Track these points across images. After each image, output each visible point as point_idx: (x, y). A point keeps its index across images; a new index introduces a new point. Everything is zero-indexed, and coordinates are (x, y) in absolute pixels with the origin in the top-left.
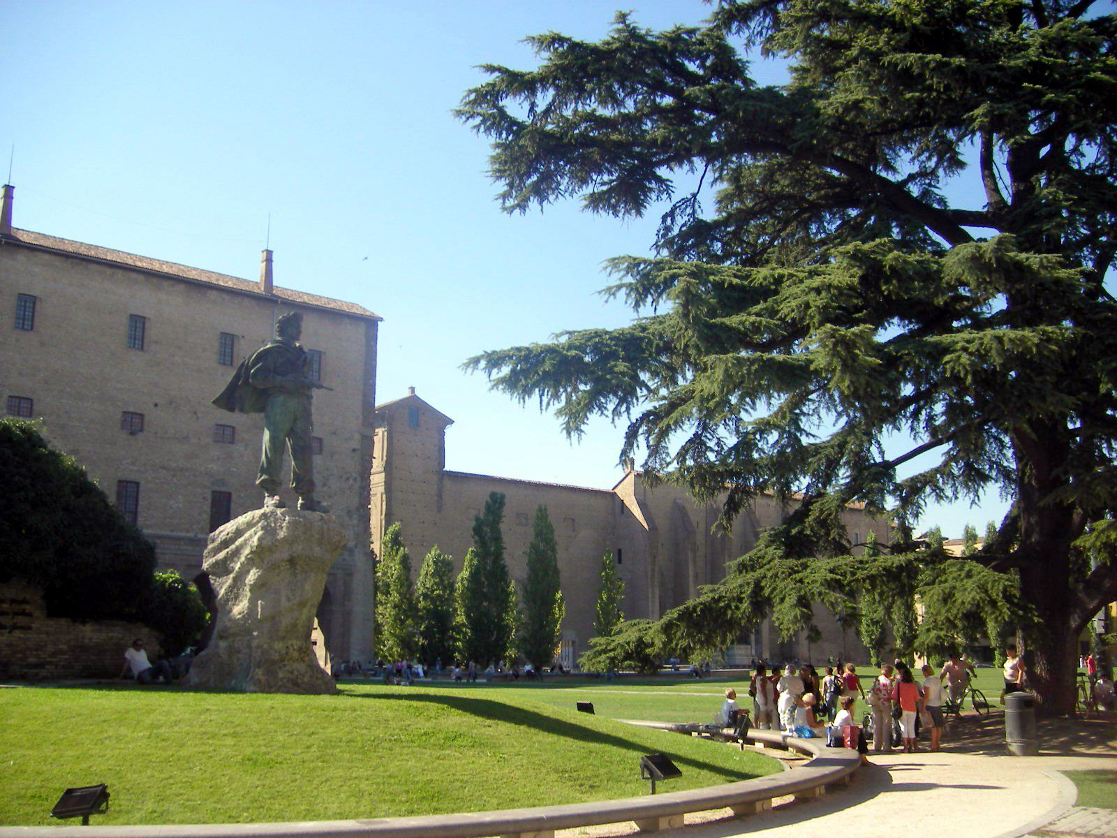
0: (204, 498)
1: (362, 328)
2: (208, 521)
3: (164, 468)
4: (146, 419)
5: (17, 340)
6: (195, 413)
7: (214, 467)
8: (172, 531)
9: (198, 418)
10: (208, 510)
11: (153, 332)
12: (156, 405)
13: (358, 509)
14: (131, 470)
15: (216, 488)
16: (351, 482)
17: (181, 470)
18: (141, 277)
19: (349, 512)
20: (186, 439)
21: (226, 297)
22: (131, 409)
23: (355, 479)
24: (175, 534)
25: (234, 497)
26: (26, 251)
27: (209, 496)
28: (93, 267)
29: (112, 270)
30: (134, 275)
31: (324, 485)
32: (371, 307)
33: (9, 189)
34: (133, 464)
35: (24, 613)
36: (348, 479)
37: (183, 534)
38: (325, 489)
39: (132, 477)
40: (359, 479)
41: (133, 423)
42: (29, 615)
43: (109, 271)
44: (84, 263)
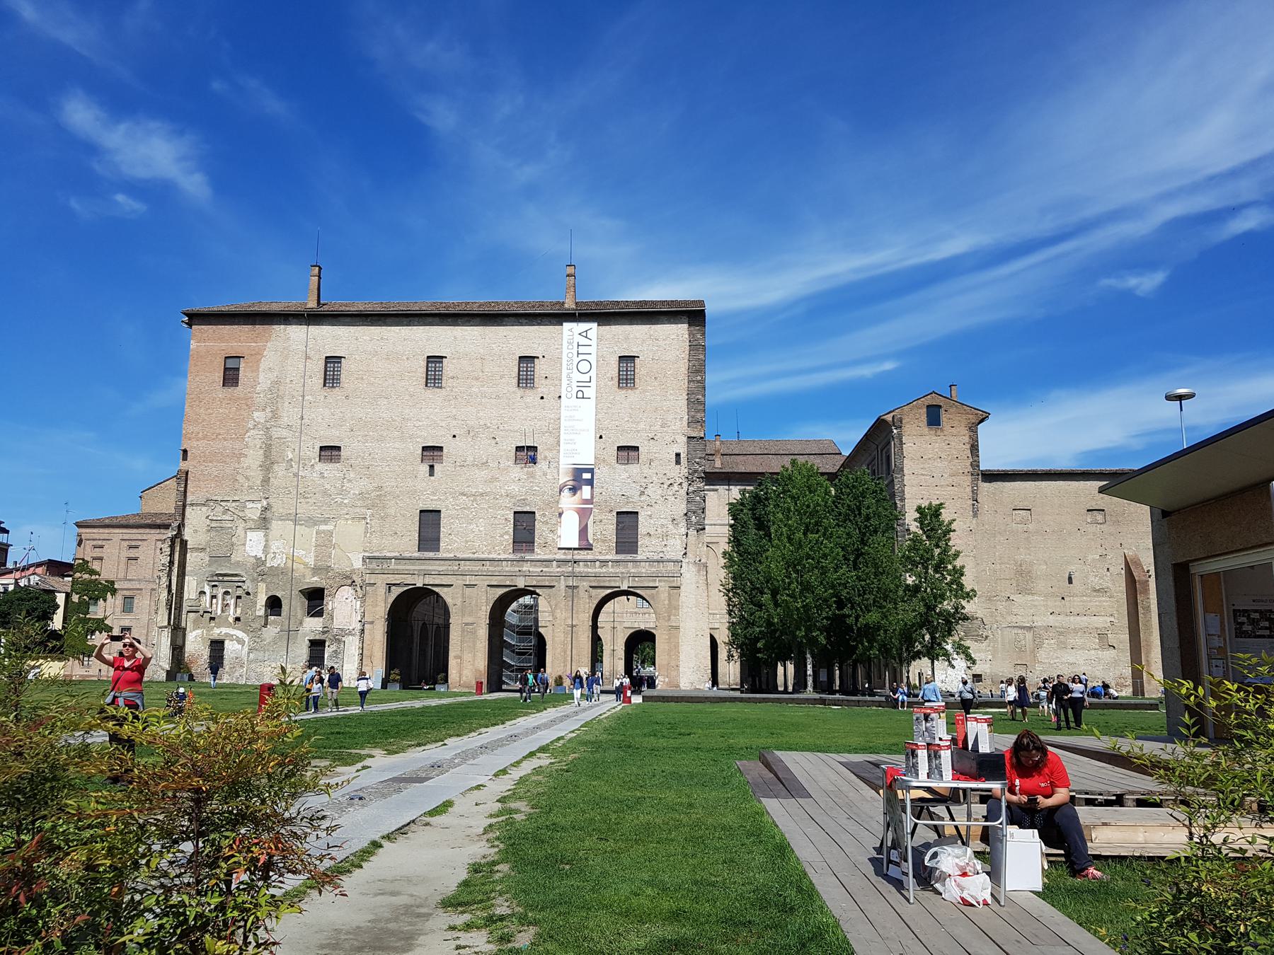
3: (463, 494)
4: (445, 450)
7: (515, 488)
15: (520, 509)
16: (676, 487)
17: (482, 495)
27: (511, 517)
28: (389, 320)
31: (642, 493)
34: (434, 494)
37: (485, 556)
40: (685, 485)
43: (405, 320)
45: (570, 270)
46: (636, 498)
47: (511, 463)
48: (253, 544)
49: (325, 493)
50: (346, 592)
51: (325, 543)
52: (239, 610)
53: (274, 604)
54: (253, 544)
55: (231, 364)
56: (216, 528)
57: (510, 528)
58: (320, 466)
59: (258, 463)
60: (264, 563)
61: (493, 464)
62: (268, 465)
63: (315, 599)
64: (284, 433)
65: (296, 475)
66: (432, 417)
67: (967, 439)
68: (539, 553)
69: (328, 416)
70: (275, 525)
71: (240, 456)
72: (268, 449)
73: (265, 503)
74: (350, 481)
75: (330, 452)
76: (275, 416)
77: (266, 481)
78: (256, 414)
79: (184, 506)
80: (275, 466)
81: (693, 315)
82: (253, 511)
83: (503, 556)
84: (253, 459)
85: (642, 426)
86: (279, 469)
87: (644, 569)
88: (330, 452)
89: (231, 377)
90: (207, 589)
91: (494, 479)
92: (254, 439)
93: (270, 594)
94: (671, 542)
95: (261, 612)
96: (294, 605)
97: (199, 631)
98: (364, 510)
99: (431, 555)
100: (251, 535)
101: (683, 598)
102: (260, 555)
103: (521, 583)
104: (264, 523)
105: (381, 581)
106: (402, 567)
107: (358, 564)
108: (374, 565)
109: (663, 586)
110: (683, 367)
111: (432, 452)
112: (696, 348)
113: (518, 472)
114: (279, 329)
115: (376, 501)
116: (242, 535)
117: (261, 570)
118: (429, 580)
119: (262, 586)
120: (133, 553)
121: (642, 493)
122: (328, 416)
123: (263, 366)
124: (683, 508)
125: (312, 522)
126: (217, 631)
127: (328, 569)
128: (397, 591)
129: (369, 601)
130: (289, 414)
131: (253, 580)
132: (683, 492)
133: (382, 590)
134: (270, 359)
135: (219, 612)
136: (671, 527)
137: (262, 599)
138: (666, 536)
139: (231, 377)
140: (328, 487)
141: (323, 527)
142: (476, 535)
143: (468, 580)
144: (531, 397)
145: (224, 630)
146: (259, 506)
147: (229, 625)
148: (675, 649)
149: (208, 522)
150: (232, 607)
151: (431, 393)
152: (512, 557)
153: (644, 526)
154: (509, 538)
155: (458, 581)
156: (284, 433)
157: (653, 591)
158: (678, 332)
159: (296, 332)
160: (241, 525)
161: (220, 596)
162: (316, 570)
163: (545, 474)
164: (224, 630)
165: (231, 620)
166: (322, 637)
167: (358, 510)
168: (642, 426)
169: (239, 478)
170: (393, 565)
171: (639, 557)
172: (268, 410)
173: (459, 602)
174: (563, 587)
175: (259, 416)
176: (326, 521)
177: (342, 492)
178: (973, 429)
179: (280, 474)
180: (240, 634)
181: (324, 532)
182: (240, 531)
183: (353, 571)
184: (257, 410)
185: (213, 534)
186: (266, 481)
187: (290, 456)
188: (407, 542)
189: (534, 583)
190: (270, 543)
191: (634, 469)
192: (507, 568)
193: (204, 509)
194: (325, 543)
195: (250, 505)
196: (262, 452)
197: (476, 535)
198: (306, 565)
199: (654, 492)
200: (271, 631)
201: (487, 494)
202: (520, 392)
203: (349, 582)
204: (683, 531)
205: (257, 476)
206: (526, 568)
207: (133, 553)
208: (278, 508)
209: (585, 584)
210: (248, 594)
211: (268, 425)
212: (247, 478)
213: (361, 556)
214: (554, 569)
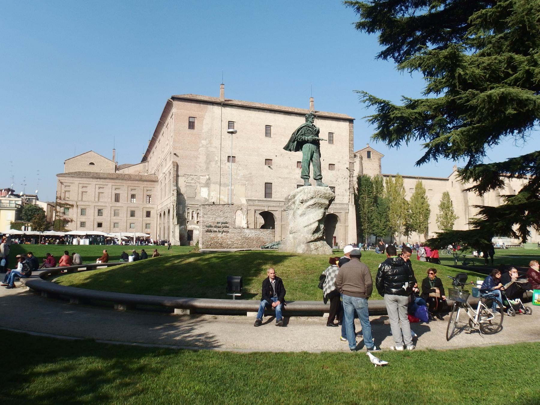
1: (347, 124)
3: (280, 177)
16: (346, 179)
34: (270, 177)
35: (226, 227)
38: (337, 182)
42: (228, 227)
45: (311, 99)
46: (335, 182)
51: (232, 193)
54: (204, 193)
55: (191, 120)
56: (188, 186)
58: (228, 164)
60: (208, 200)
62: (208, 162)
64: (214, 150)
67: (378, 163)
69: (230, 145)
70: (212, 186)
71: (197, 158)
73: (208, 177)
75: (231, 158)
76: (210, 142)
77: (207, 168)
78: (203, 141)
79: (177, 176)
81: (351, 121)
82: (203, 180)
84: (202, 159)
85: (336, 157)
86: (213, 164)
88: (231, 158)
89: (191, 125)
91: (290, 173)
92: (202, 150)
94: (345, 197)
98: (245, 182)
99: (269, 199)
100: (202, 189)
102: (207, 197)
104: (207, 185)
105: (253, 209)
107: (244, 201)
108: (250, 203)
109: (343, 212)
111: (268, 161)
112: (351, 132)
114: (210, 107)
115: (249, 179)
122: (230, 145)
123: (205, 122)
125: (226, 185)
130: (216, 142)
134: (207, 120)
135: (191, 219)
138: (343, 195)
139: (191, 125)
146: (205, 178)
147: (194, 224)
151: (267, 139)
155: (280, 209)
158: (346, 125)
159: (217, 109)
160: (199, 185)
165: (196, 222)
168: (336, 157)
169: (198, 167)
170: (257, 203)
172: (207, 140)
173: (280, 217)
175: (204, 142)
178: (380, 159)
179: (213, 166)
182: (198, 188)
183: (242, 205)
185: (188, 188)
186: (207, 168)
187: (217, 159)
188: (260, 194)
193: (183, 178)
194: (232, 193)
195: (201, 177)
199: (340, 180)
204: (348, 194)
208: (213, 179)
211: (208, 146)
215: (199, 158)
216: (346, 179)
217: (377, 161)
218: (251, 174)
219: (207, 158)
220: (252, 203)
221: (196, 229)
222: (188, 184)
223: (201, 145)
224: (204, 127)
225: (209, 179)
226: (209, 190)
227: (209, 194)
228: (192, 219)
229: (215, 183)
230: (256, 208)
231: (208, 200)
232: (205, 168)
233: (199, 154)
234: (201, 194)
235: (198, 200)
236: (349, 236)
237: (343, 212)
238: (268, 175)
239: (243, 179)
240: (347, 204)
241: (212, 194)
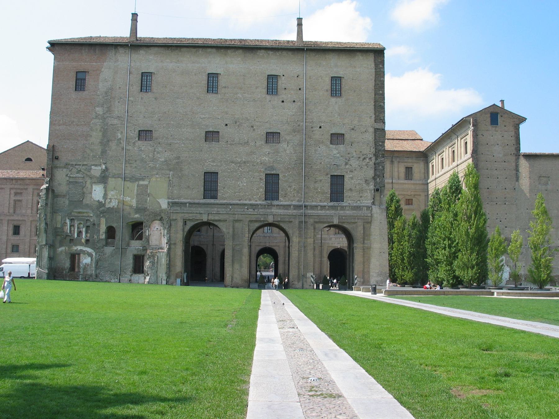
0: (260, 179)
2: (264, 192)
3: (232, 162)
4: (221, 134)
5: (142, 98)
6: (252, 127)
8: (240, 200)
9: (254, 130)
10: (264, 186)
11: (222, 81)
12: (226, 125)
13: (374, 178)
14: (212, 166)
15: (269, 172)
16: (367, 160)
17: (245, 162)
18: (214, 50)
19: (366, 181)
20: (247, 143)
21: (271, 53)
22: (211, 129)
23: (370, 158)
24: (241, 202)
25: (280, 176)
26: (145, 49)
27: (263, 177)
28: (183, 49)
29: (196, 49)
30: (209, 50)
31: (346, 164)
32: (383, 44)
33: (135, 17)
34: (213, 162)
36: (364, 158)
37: (247, 202)
38: (347, 167)
39: (213, 170)
40: (374, 158)
41: (211, 136)
44: (179, 48)
46: (343, 166)
47: (263, 142)
48: (97, 193)
49: (142, 160)
50: (156, 225)
51: (143, 192)
52: (88, 235)
53: (111, 232)
54: (97, 193)
55: (80, 76)
56: (73, 183)
57: (263, 184)
59: (99, 140)
60: (104, 205)
61: (252, 144)
62: (105, 143)
63: (137, 229)
64: (116, 121)
65: (123, 149)
66: (211, 111)
68: (282, 201)
69: (143, 111)
70: (111, 182)
72: (105, 132)
73: (104, 167)
74: (158, 153)
75: (145, 134)
76: (109, 110)
77: (104, 152)
78: (97, 109)
80: (110, 143)
82: (96, 171)
83: (259, 202)
84: (96, 137)
86: (113, 145)
87: (348, 212)
88: (145, 134)
90: (68, 222)
93: (109, 225)
95: (103, 237)
96: (122, 233)
97: (63, 248)
98: (168, 172)
99: (212, 201)
100: (95, 187)
101: (372, 230)
102: (101, 199)
103: (270, 219)
104: (103, 179)
105: (179, 218)
106: (193, 209)
110: (371, 84)
113: (267, 149)
114: (111, 53)
115: (175, 167)
116: (90, 187)
117: (101, 209)
118: (211, 217)
119: (103, 221)
120: (18, 198)
121: (346, 164)
124: (371, 173)
125: (133, 179)
126: (75, 248)
127: (145, 209)
128: (190, 225)
129: (173, 230)
130: (118, 109)
131: (98, 216)
132: (372, 163)
133: (180, 224)
135: (76, 236)
136: (364, 185)
137: (103, 228)
138: (361, 191)
140: (144, 156)
141: (141, 183)
142: (242, 189)
143: (237, 217)
144: (276, 100)
145: (79, 248)
147: (82, 245)
148: (366, 260)
149: (68, 178)
150: (84, 233)
151: (211, 97)
152: (264, 203)
153: (348, 183)
154: (262, 190)
156: (116, 121)
157: (354, 225)
160: (89, 181)
161: (76, 225)
162: (138, 210)
163: (285, 151)
164: (79, 248)
165: (83, 241)
166: (143, 253)
167: (163, 172)
169: (88, 151)
171: (344, 204)
174: (297, 222)
175: (99, 110)
176: (143, 179)
177: (153, 160)
180: (89, 250)
181: (142, 185)
183: (162, 211)
184: (98, 106)
186: (104, 152)
187: (120, 136)
188: (195, 193)
189: (279, 219)
190: (108, 192)
191: (341, 147)
192: (262, 211)
193: (65, 170)
194: (143, 192)
196: (101, 134)
197: (242, 189)
198: (131, 206)
199: (354, 163)
200: (109, 250)
201: (248, 162)
202: (268, 97)
203: (159, 218)
205: (98, 149)
206: (274, 210)
207: (18, 198)
209: (312, 221)
210: (94, 224)
212: (91, 150)
213: (166, 201)
214: (291, 212)
215: (91, 136)
216: (367, 160)
217: (512, 129)
218: (178, 158)
219: (104, 136)
220: (179, 208)
221: (83, 252)
222: (71, 180)
223: (94, 117)
224: (101, 85)
225: (104, 171)
226: (105, 188)
227: (105, 196)
228: (78, 235)
229: (115, 176)
230: (187, 216)
231: (104, 205)
232: (99, 153)
233: (92, 130)
234: (93, 195)
235: (87, 206)
236: (372, 266)
237: (360, 223)
238: (211, 158)
239: (165, 167)
240: (368, 208)
241: (111, 194)
